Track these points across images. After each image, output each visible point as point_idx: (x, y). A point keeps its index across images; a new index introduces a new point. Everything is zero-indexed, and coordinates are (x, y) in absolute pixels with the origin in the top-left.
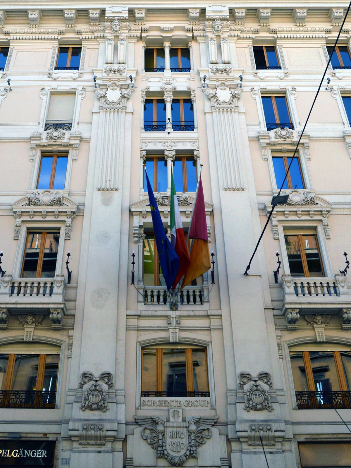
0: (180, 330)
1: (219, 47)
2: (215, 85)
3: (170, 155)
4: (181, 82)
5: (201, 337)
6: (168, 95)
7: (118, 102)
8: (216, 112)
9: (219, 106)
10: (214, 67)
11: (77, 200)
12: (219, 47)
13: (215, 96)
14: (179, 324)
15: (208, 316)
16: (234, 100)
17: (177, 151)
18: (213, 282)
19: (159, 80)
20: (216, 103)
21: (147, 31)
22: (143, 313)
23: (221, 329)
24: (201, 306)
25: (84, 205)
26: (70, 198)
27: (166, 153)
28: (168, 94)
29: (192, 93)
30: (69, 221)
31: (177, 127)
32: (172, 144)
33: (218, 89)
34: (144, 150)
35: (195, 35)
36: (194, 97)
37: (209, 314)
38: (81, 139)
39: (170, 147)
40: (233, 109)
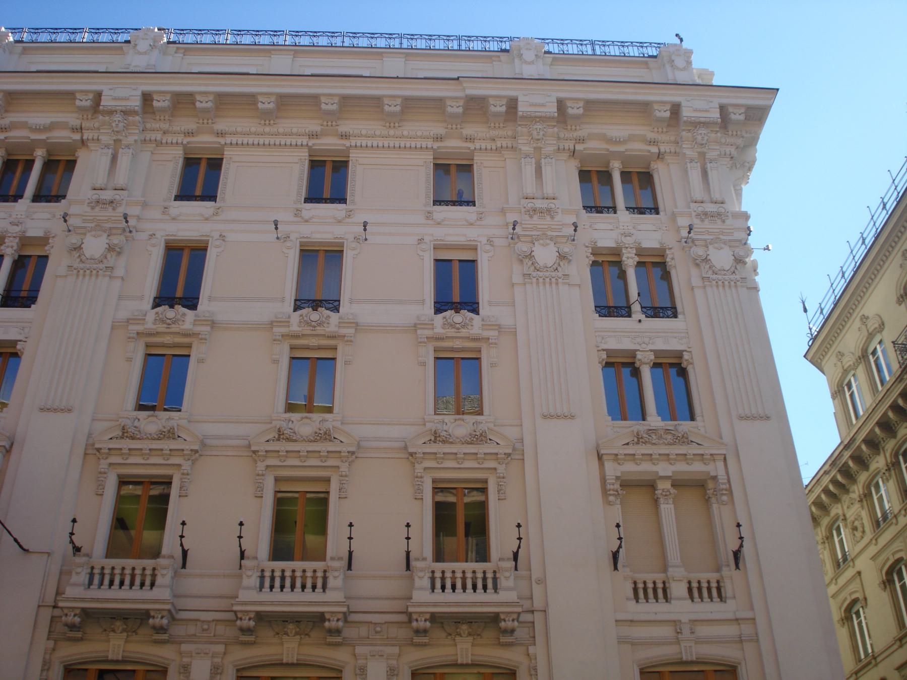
0: (696, 643)
1: (705, 173)
2: (705, 240)
3: (646, 360)
4: (647, 233)
5: (729, 653)
6: (630, 255)
7: (555, 267)
8: (711, 286)
9: (715, 276)
10: (700, 209)
11: (512, 433)
12: (705, 173)
13: (706, 260)
14: (692, 633)
15: (737, 620)
16: (738, 267)
17: (657, 353)
18: (737, 567)
19: (610, 227)
20: (710, 272)
21: (581, 140)
22: (636, 618)
23: (756, 639)
24: (722, 605)
25: (522, 440)
26: (496, 429)
27: (639, 356)
28: (629, 253)
29: (668, 252)
30: (501, 469)
31: (654, 312)
32: (646, 340)
33: (710, 247)
34: (604, 350)
35: (662, 150)
36: (673, 259)
37: (738, 617)
38: (499, 328)
39: (644, 346)
40: (738, 283)
